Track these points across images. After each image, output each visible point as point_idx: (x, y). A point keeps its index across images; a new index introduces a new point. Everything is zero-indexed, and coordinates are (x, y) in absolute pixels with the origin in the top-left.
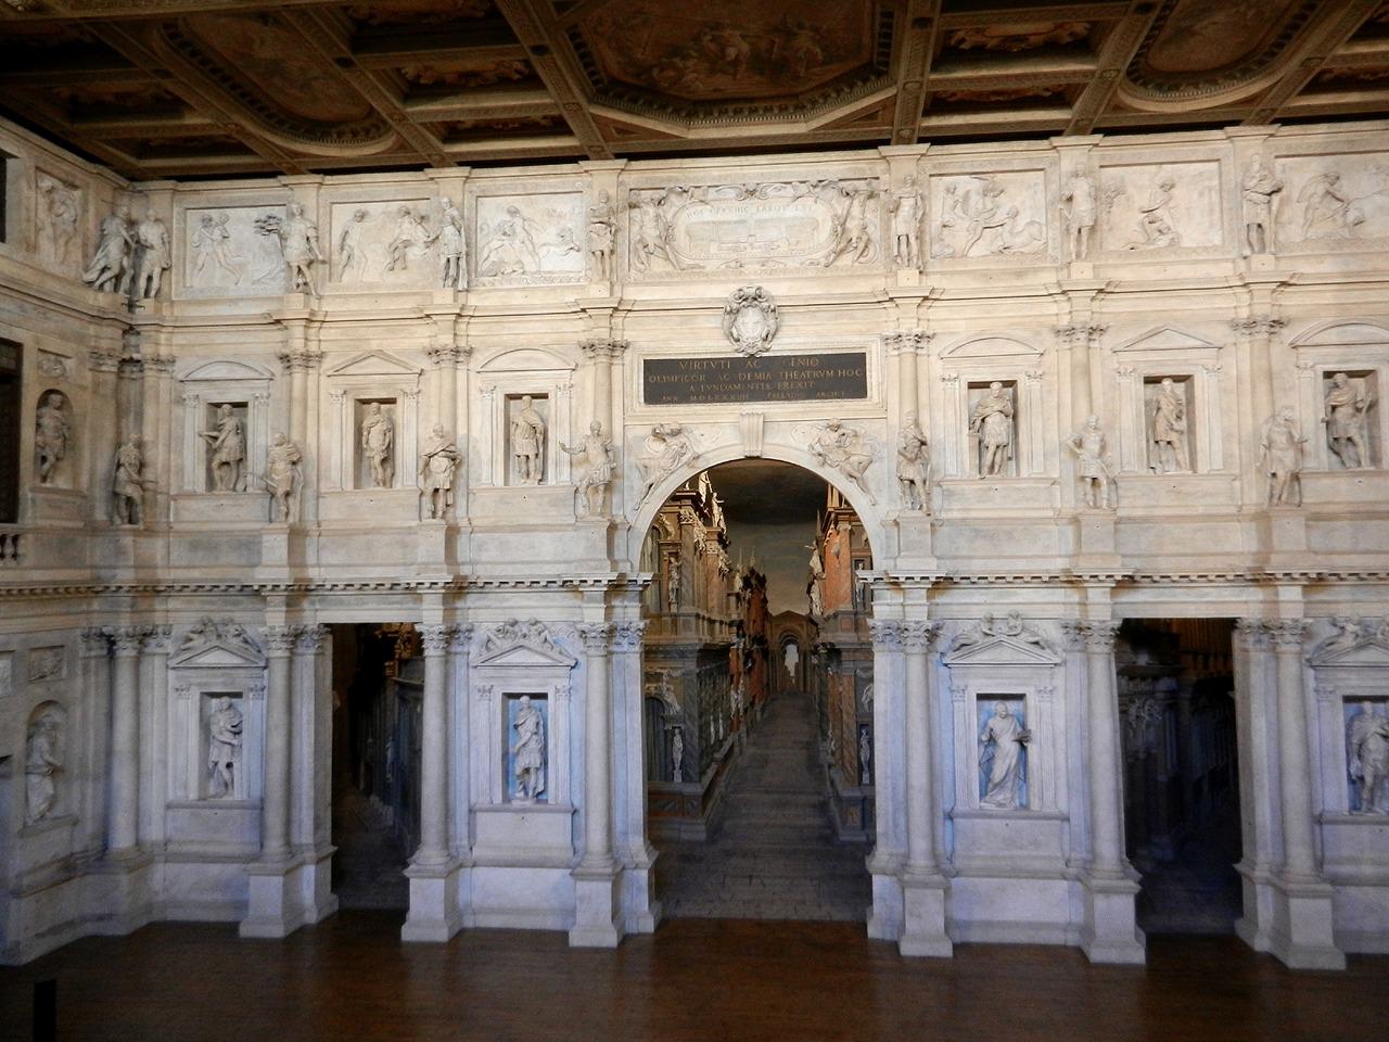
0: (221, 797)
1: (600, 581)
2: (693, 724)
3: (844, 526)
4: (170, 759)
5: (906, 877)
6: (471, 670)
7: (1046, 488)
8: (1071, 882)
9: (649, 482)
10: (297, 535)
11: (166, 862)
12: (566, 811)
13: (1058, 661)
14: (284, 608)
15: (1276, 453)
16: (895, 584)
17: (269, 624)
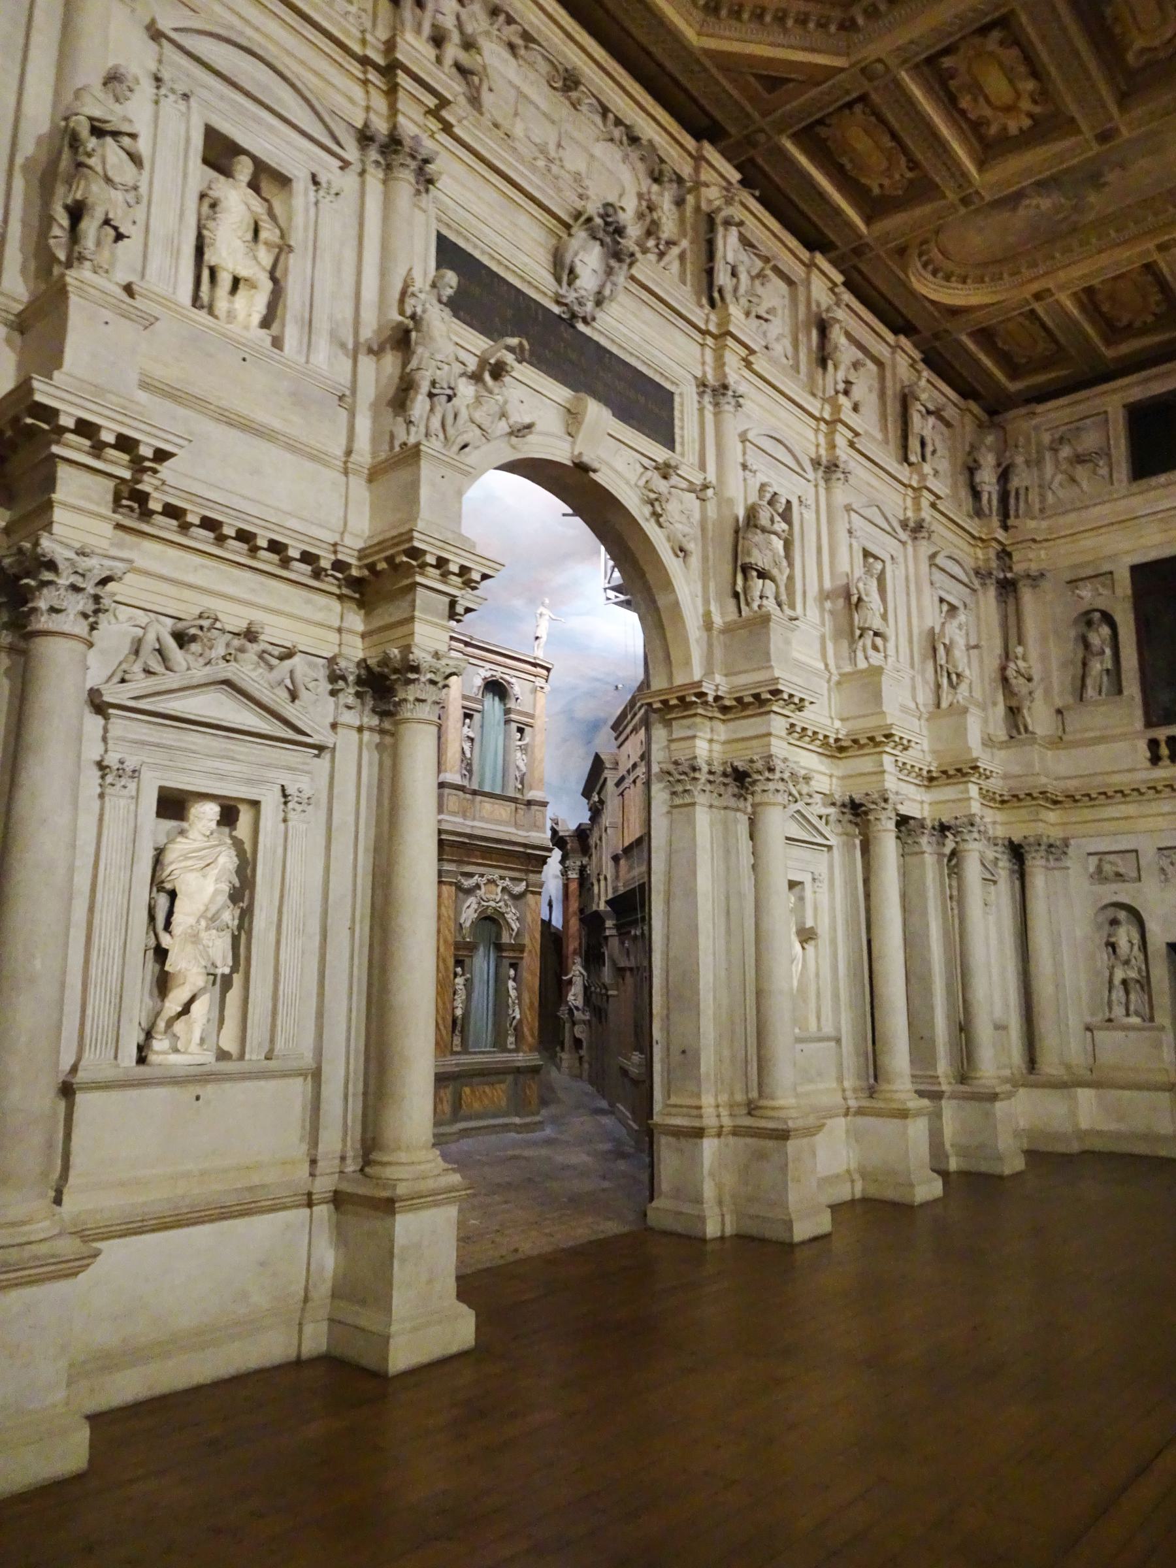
5: (791, 1124)
8: (849, 1118)
9: (465, 438)
15: (959, 653)
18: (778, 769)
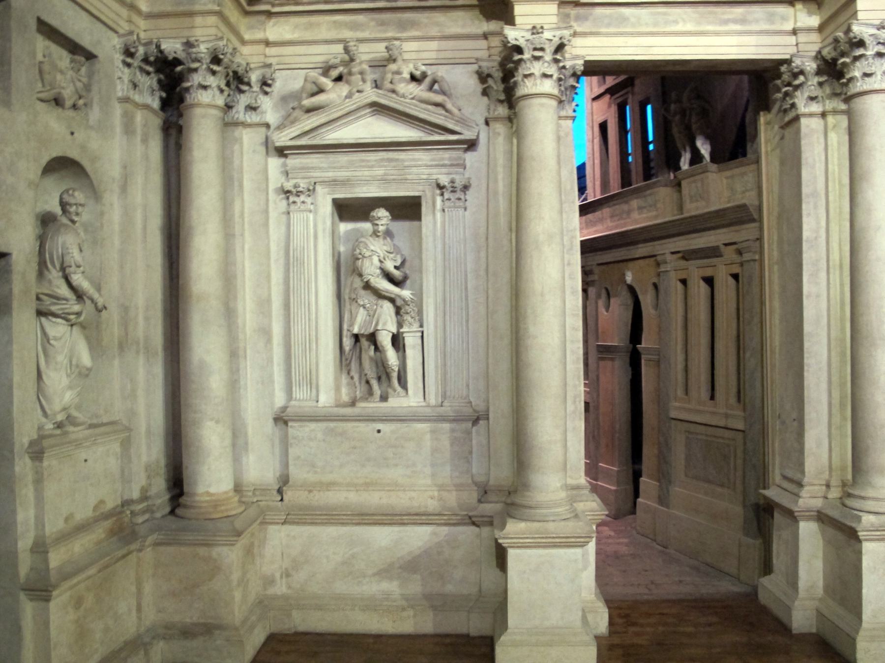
0: (384, 398)
11: (284, 523)
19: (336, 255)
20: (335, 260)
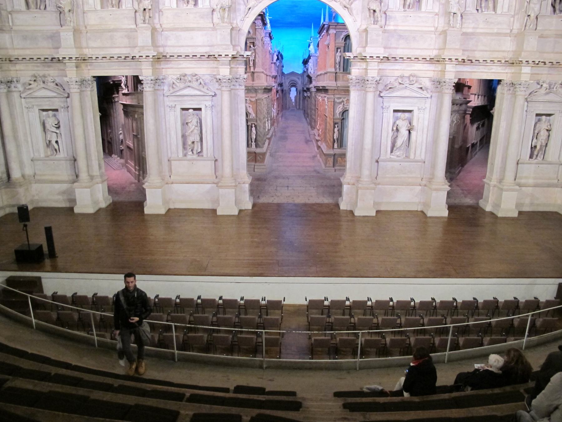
1: (228, 55)
2: (261, 122)
3: (332, 31)
4: (29, 140)
5: (360, 185)
6: (165, 98)
7: (433, 17)
9: (249, 7)
10: (76, 32)
11: (35, 183)
12: (213, 160)
13: (429, 96)
14: (75, 69)
16: (364, 59)
17: (68, 77)
18: (369, 80)
19: (42, 121)
20: (42, 123)
